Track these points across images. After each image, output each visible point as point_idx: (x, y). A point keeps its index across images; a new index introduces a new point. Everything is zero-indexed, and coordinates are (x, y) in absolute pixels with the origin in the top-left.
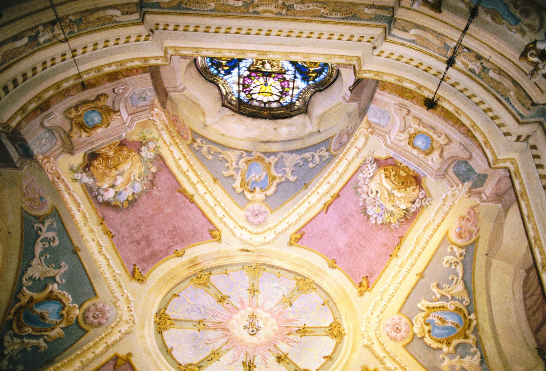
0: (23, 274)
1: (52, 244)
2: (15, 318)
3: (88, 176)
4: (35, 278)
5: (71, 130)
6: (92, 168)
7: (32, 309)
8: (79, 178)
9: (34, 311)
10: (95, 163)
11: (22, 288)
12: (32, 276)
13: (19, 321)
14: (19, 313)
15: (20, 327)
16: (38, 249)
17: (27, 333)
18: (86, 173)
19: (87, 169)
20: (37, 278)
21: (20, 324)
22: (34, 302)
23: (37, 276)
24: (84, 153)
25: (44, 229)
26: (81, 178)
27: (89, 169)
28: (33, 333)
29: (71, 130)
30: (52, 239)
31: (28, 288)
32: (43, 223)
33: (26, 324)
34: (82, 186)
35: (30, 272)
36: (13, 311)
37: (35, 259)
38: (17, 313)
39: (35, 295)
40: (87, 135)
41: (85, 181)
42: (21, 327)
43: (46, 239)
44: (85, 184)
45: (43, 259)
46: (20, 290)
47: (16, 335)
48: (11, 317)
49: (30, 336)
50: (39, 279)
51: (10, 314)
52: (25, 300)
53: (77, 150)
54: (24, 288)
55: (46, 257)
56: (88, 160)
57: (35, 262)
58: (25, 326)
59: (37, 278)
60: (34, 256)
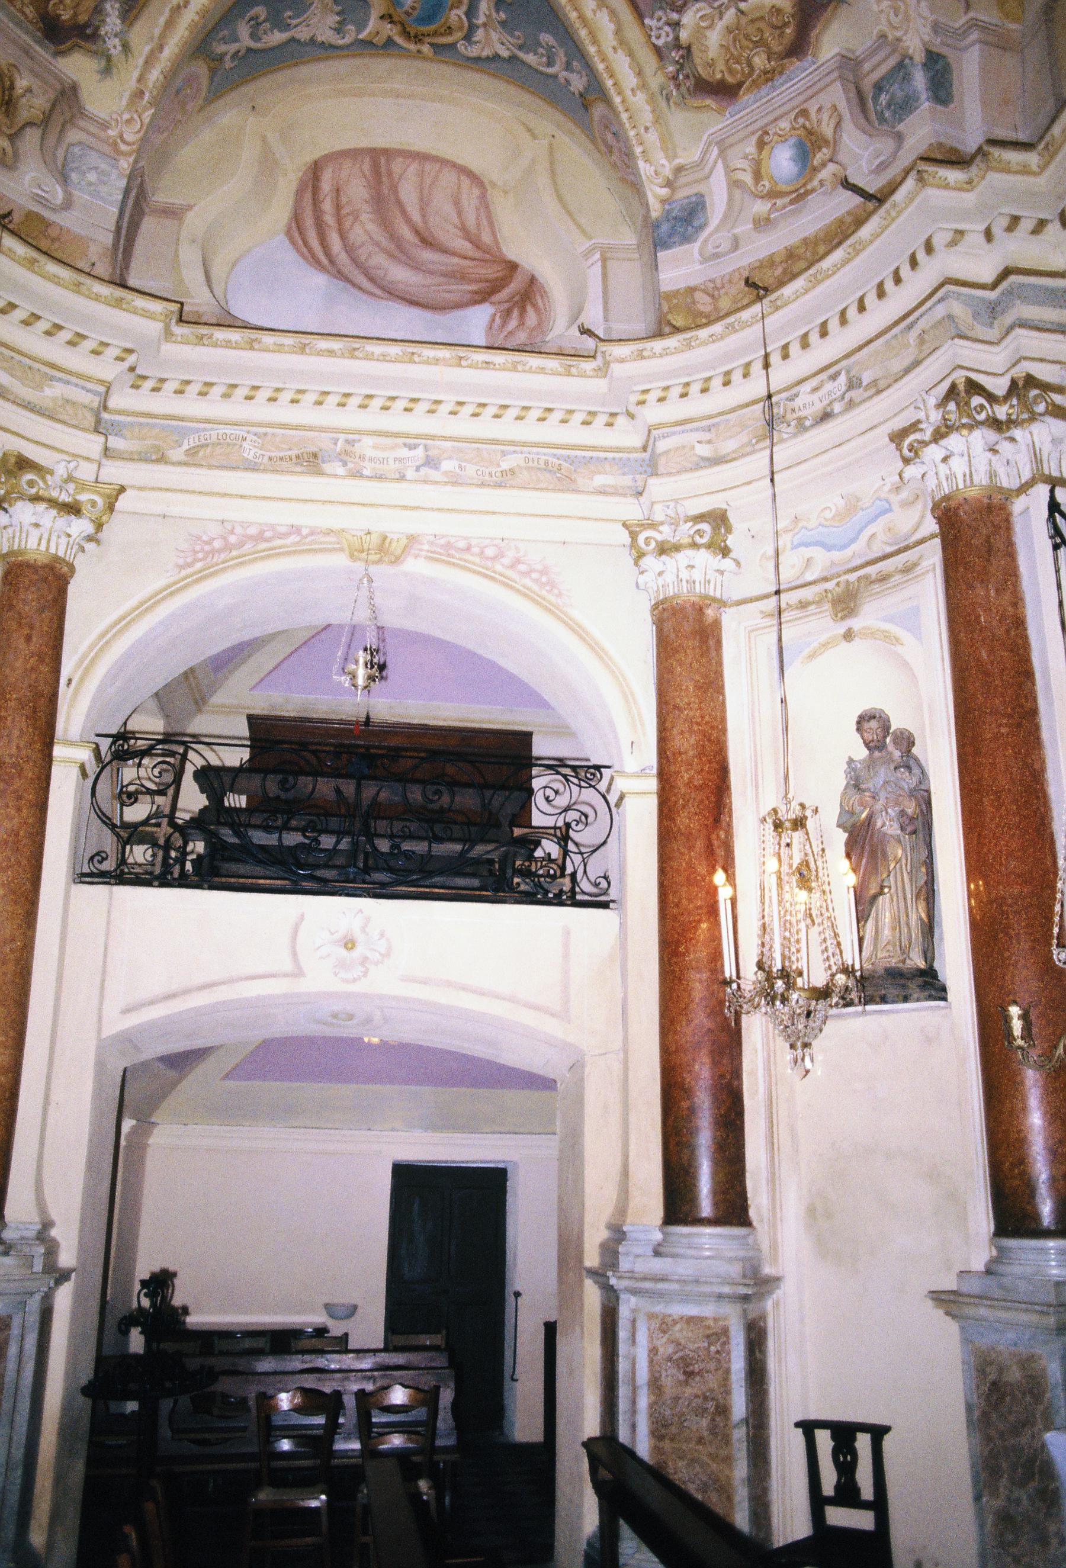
0: (332, 47)
1: (262, 18)
2: (427, 39)
3: (104, 21)
4: (338, 23)
5: (30, 124)
6: (82, 18)
7: (408, 14)
8: (116, 41)
9: (413, 8)
10: (66, 16)
11: (363, 42)
12: (335, 29)
13: (435, 33)
14: (416, 36)
15: (449, 30)
16: (278, 37)
17: (463, 17)
18: (98, 28)
19: (89, 31)
20: (338, 18)
21: (442, 30)
22: (391, 11)
23: (333, 19)
24: (59, 59)
25: (233, 48)
26: (115, 36)
27: (87, 25)
28: (464, 8)
29: (30, 124)
30: (252, 23)
31: (359, 31)
32: (221, 58)
33: (443, 20)
34: (131, 24)
35: (326, 35)
36: (412, 47)
37: (298, 36)
38: (418, 39)
39: (374, 15)
40: (17, 75)
41: (118, 21)
42: (449, 28)
43: (254, 36)
44: (123, 21)
45: (294, 22)
46: (368, 43)
47: (468, 38)
48: (426, 49)
49: (471, 13)
50: (338, 14)
51: (419, 51)
52: (389, 30)
53: (61, 81)
54: (361, 37)
55: (290, 17)
56: (68, 38)
57: (303, 34)
58: (447, 20)
59: (338, 18)
60: (293, 40)
